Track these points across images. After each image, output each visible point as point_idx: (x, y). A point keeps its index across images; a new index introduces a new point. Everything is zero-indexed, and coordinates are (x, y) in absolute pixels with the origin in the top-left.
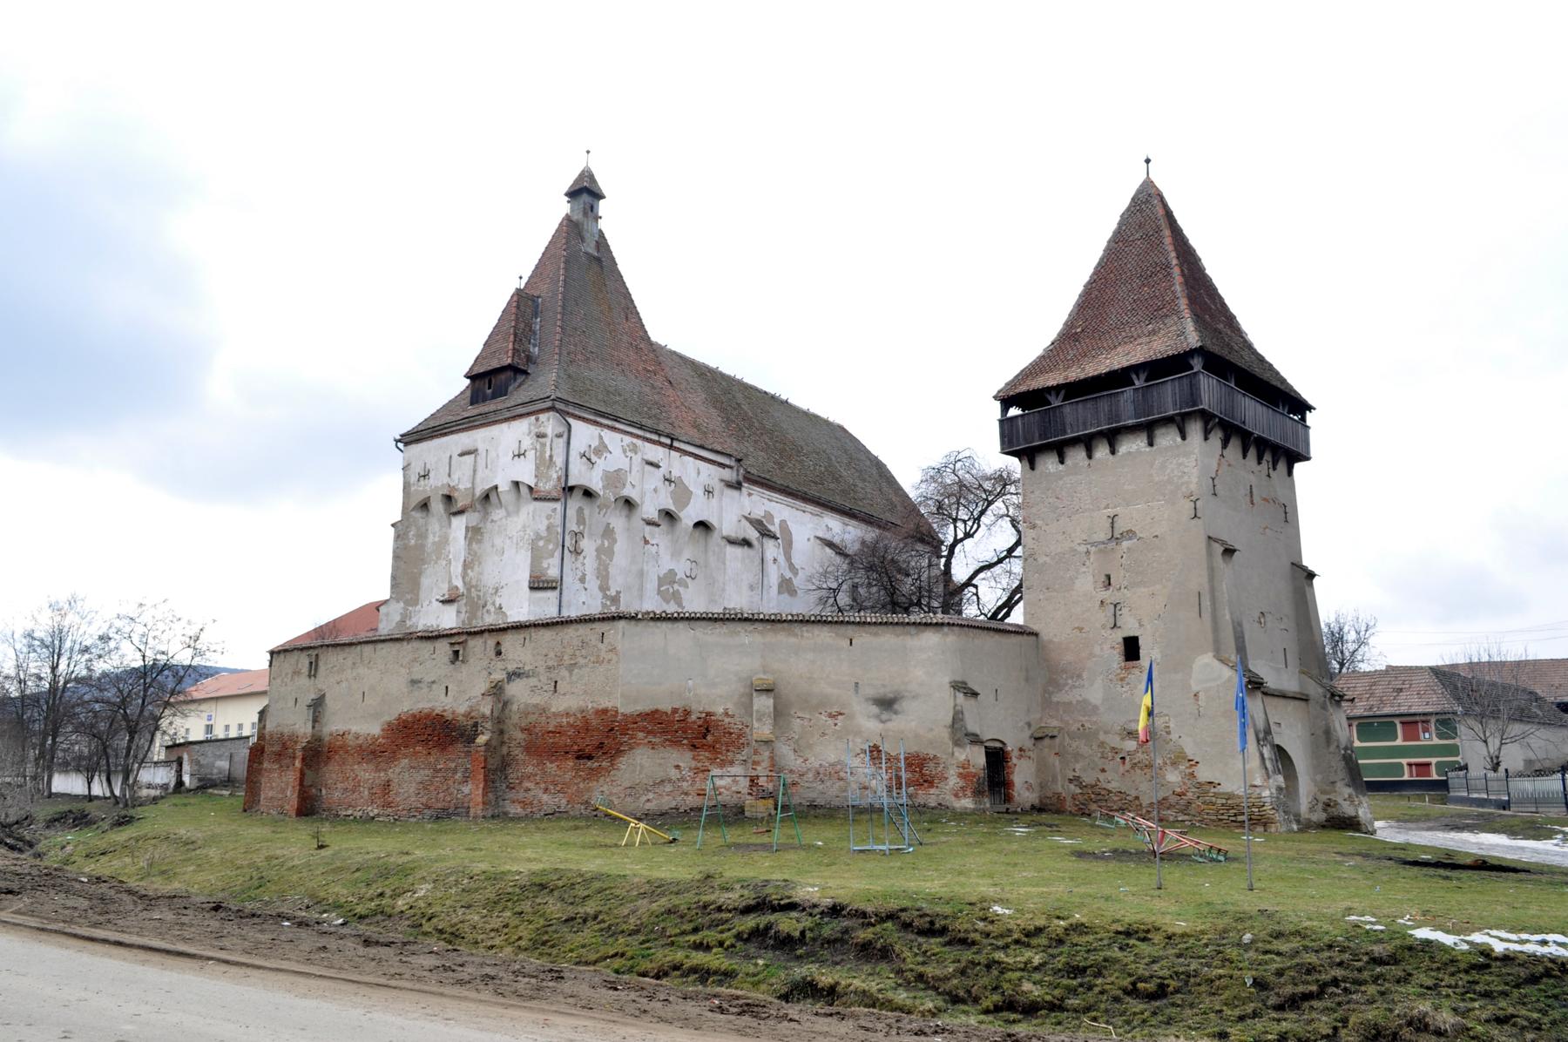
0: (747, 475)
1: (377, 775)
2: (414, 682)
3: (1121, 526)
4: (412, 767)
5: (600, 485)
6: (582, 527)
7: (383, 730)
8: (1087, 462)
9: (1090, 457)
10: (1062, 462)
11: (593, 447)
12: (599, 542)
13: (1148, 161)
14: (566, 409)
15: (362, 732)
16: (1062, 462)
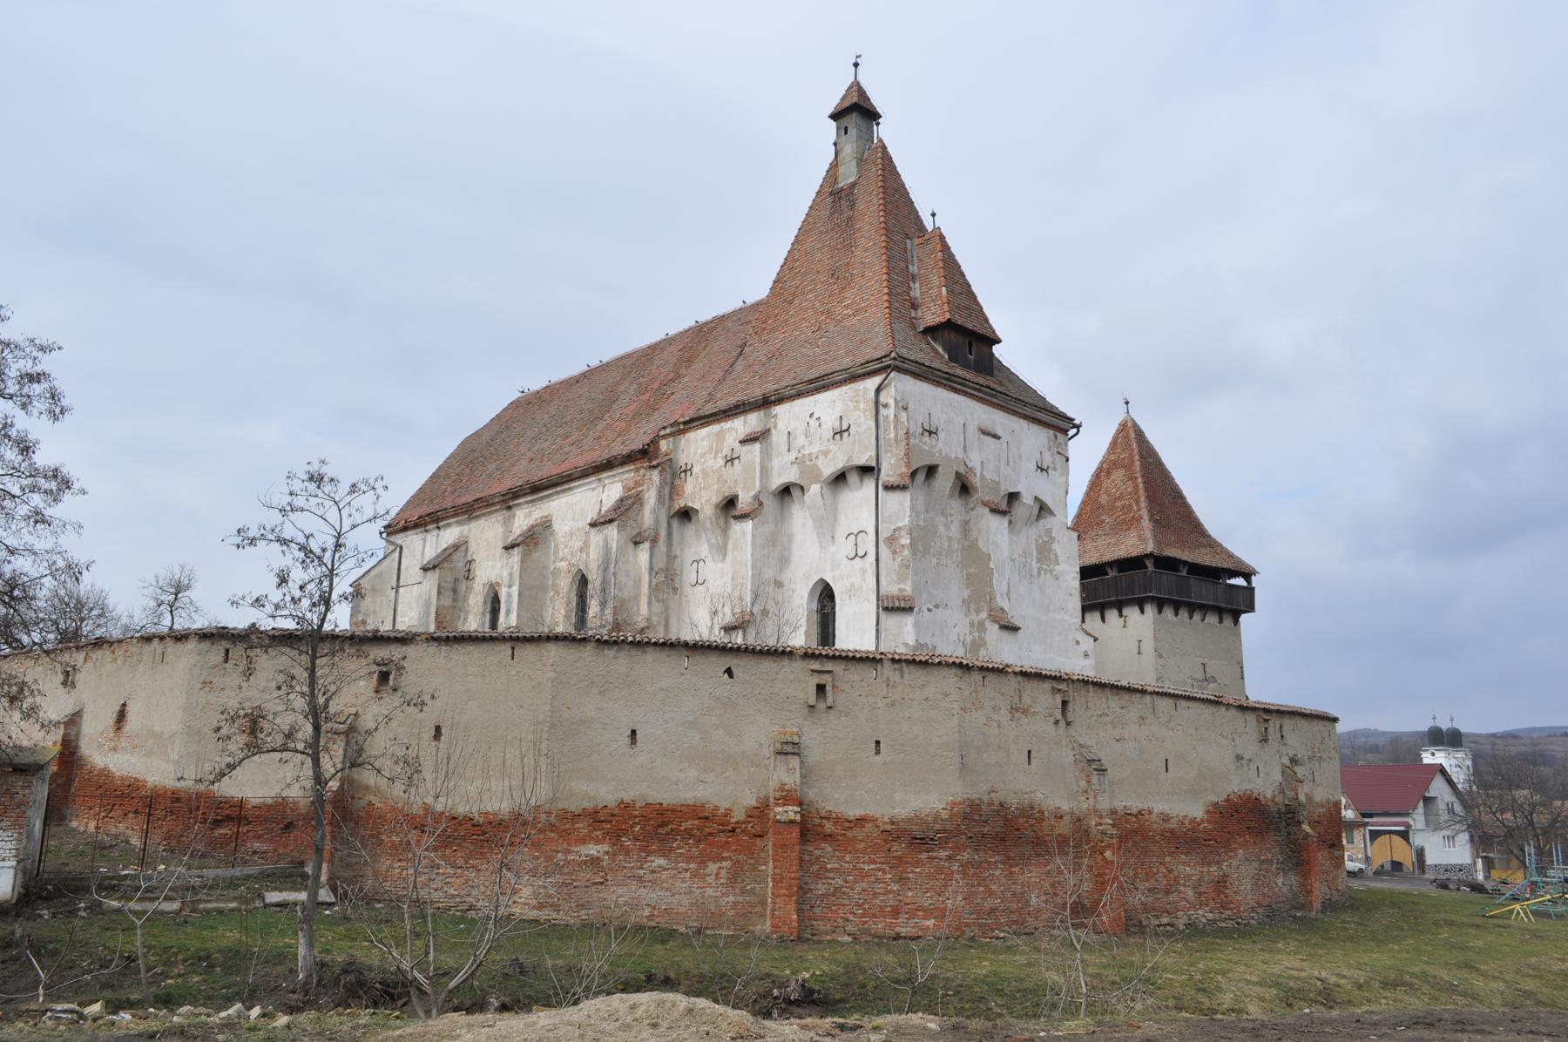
1: (1205, 869)
2: (1239, 758)
3: (1210, 673)
4: (1246, 859)
7: (1208, 812)
8: (1188, 621)
9: (1191, 618)
10: (1176, 615)
13: (1127, 403)
15: (1174, 813)
16: (1176, 615)
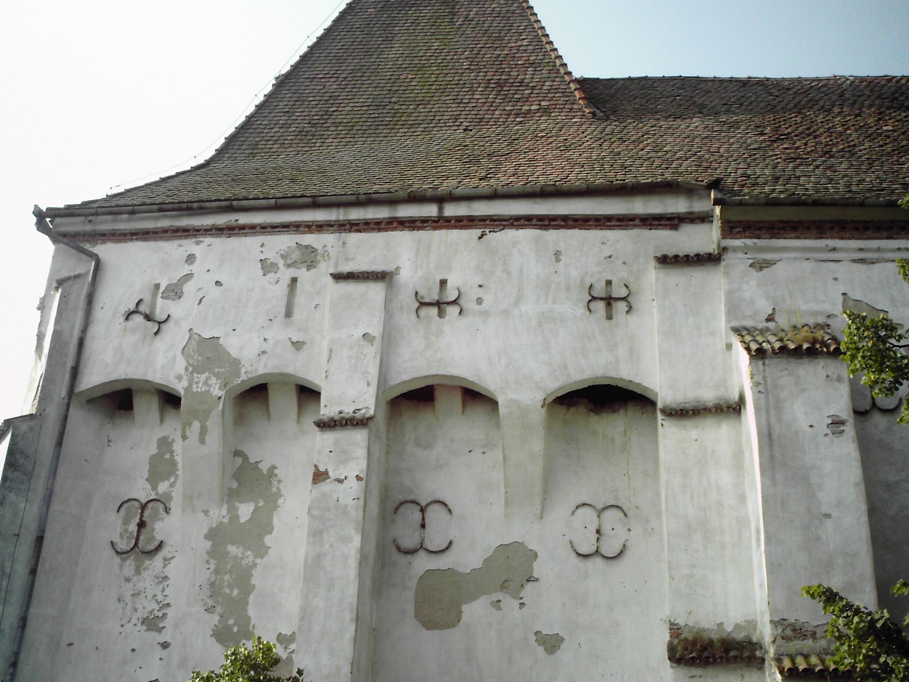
0: (736, 215)
5: (181, 365)
6: (163, 487)
11: (162, 289)
12: (219, 514)
14: (88, 228)
